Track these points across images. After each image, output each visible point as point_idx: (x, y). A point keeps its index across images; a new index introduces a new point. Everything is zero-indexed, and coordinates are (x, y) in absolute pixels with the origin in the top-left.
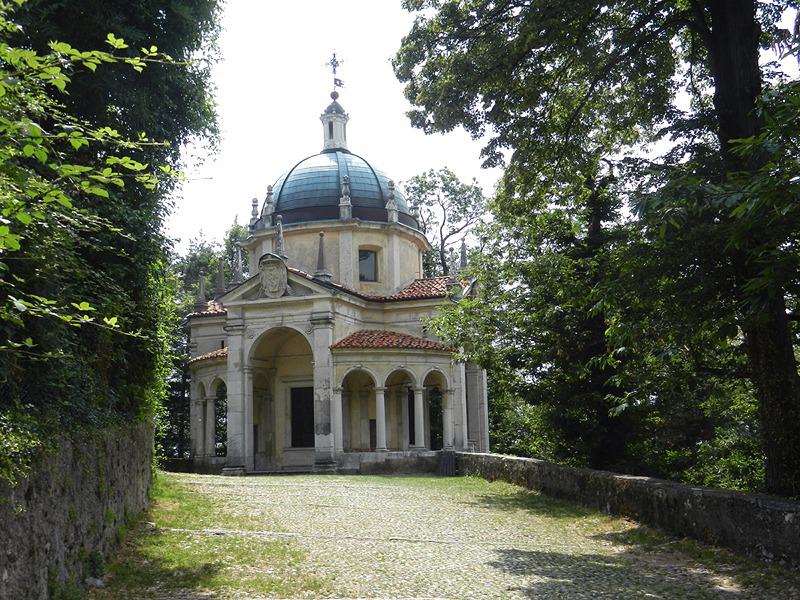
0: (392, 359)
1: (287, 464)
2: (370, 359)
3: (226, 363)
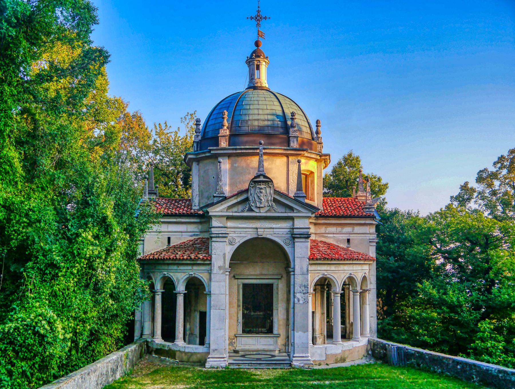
0: (346, 267)
1: (240, 348)
2: (333, 268)
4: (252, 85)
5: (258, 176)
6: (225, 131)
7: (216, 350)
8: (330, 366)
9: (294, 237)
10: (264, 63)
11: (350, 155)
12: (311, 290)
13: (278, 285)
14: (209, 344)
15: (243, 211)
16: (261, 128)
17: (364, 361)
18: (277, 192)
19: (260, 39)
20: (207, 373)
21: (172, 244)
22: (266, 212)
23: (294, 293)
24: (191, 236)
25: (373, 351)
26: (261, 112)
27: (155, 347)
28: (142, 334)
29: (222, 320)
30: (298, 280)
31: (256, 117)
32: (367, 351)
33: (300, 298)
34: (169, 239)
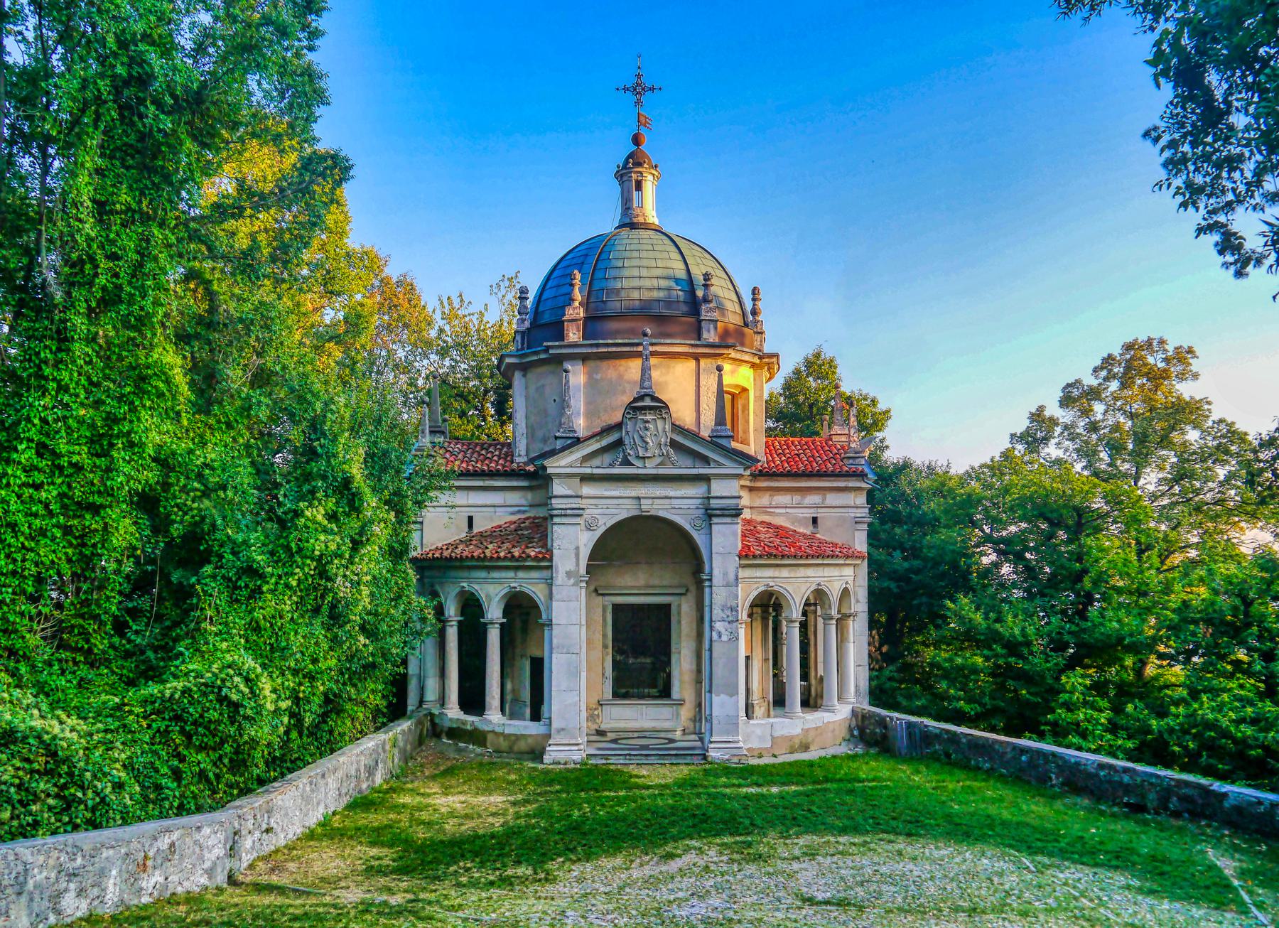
0: (810, 572)
1: (609, 726)
2: (785, 573)
4: (628, 221)
5: (641, 398)
6: (576, 311)
7: (563, 729)
8: (780, 760)
9: (710, 514)
10: (650, 177)
11: (817, 355)
12: (743, 616)
13: (679, 606)
14: (550, 719)
15: (611, 466)
16: (646, 304)
17: (843, 749)
18: (677, 428)
19: (643, 131)
20: (546, 772)
21: (476, 530)
22: (657, 467)
23: (711, 621)
24: (513, 513)
25: (862, 730)
26: (644, 273)
27: (447, 724)
28: (421, 702)
29: (574, 673)
30: (718, 596)
31: (636, 283)
32: (851, 730)
33: (723, 631)
34: (470, 519)
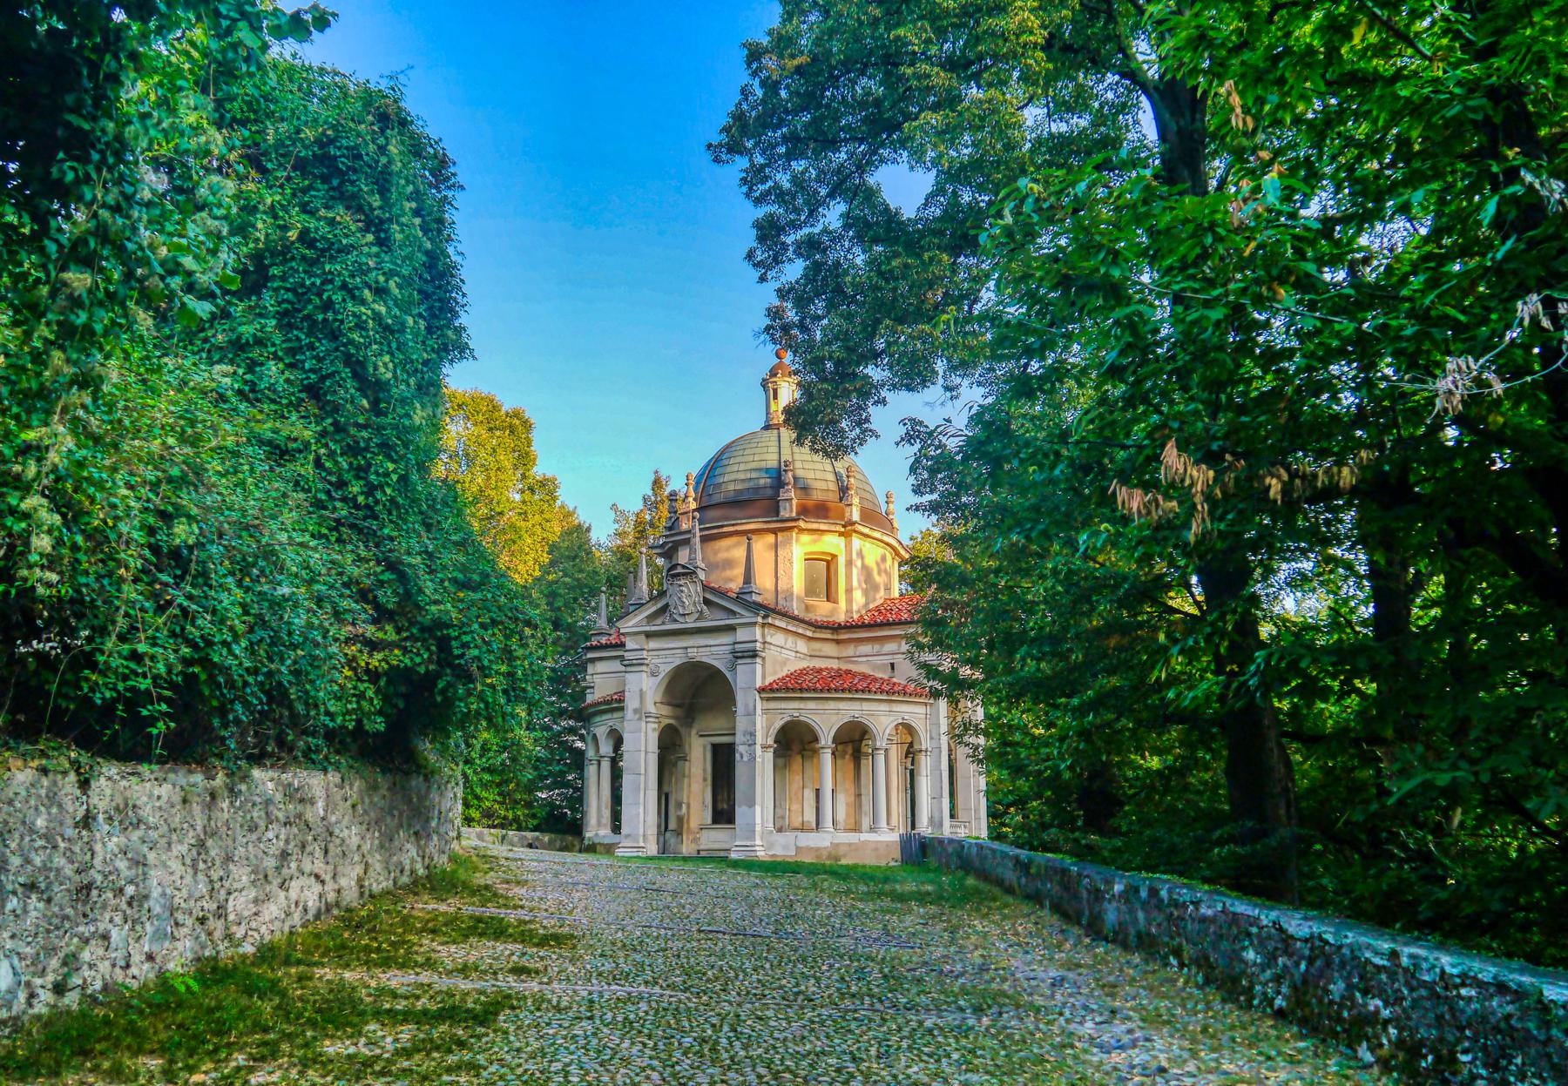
0: (842, 705)
2: (811, 705)
3: (622, 709)
18: (706, 587)
31: (733, 477)
